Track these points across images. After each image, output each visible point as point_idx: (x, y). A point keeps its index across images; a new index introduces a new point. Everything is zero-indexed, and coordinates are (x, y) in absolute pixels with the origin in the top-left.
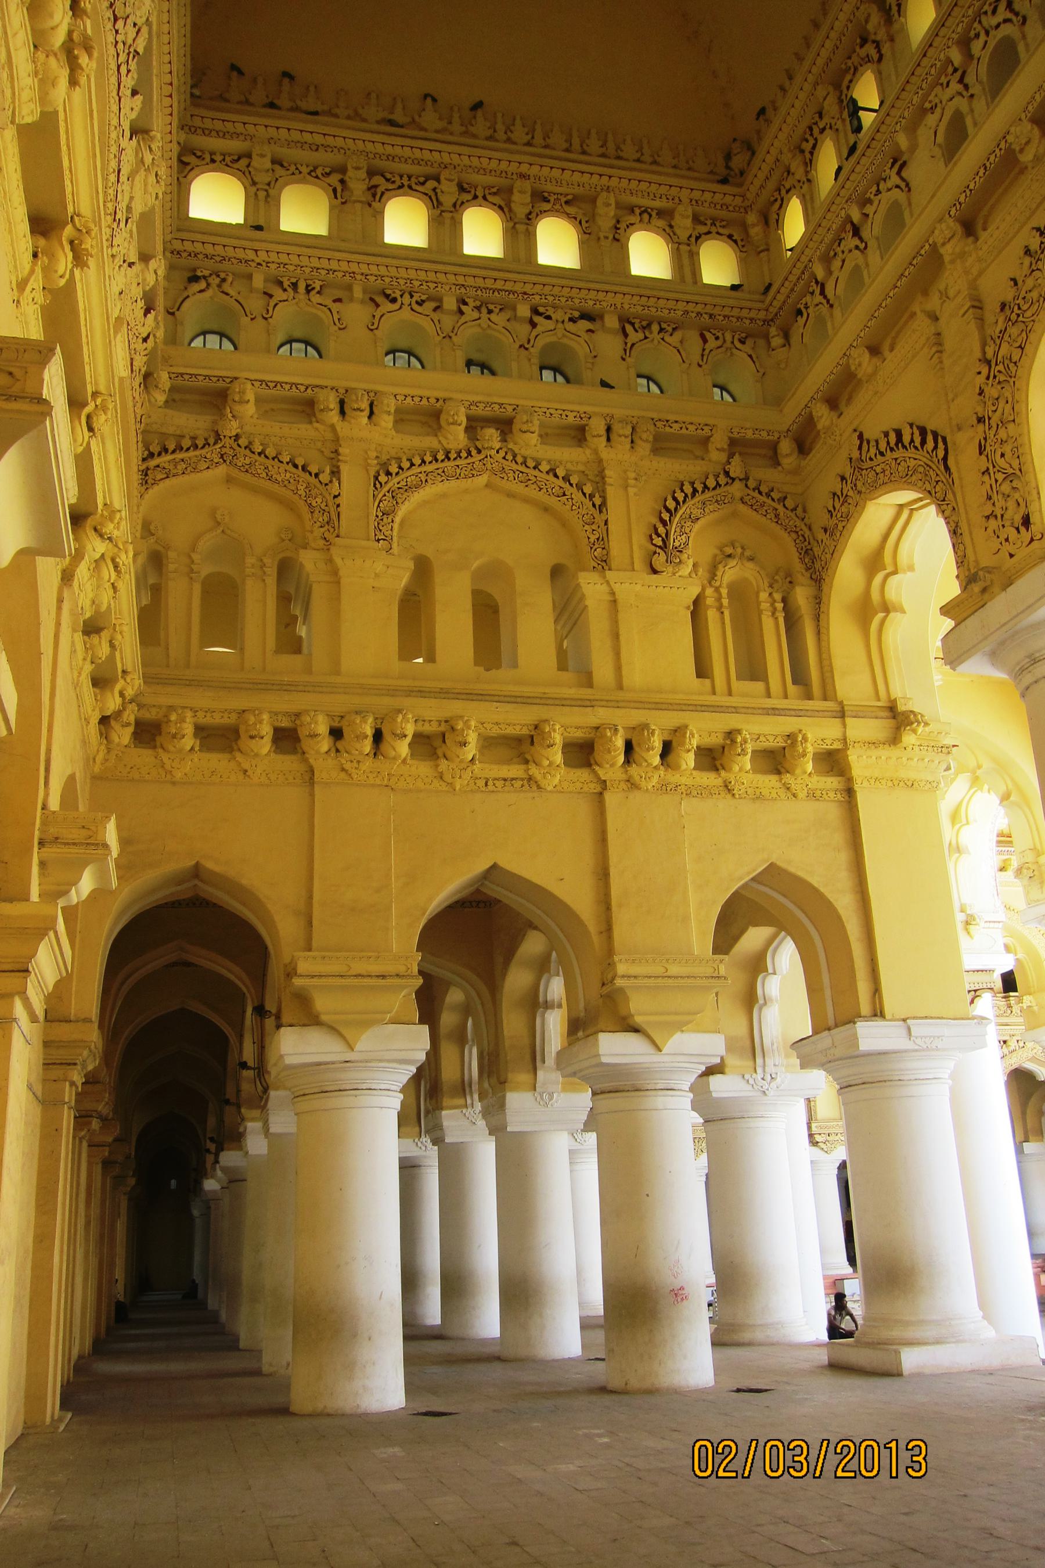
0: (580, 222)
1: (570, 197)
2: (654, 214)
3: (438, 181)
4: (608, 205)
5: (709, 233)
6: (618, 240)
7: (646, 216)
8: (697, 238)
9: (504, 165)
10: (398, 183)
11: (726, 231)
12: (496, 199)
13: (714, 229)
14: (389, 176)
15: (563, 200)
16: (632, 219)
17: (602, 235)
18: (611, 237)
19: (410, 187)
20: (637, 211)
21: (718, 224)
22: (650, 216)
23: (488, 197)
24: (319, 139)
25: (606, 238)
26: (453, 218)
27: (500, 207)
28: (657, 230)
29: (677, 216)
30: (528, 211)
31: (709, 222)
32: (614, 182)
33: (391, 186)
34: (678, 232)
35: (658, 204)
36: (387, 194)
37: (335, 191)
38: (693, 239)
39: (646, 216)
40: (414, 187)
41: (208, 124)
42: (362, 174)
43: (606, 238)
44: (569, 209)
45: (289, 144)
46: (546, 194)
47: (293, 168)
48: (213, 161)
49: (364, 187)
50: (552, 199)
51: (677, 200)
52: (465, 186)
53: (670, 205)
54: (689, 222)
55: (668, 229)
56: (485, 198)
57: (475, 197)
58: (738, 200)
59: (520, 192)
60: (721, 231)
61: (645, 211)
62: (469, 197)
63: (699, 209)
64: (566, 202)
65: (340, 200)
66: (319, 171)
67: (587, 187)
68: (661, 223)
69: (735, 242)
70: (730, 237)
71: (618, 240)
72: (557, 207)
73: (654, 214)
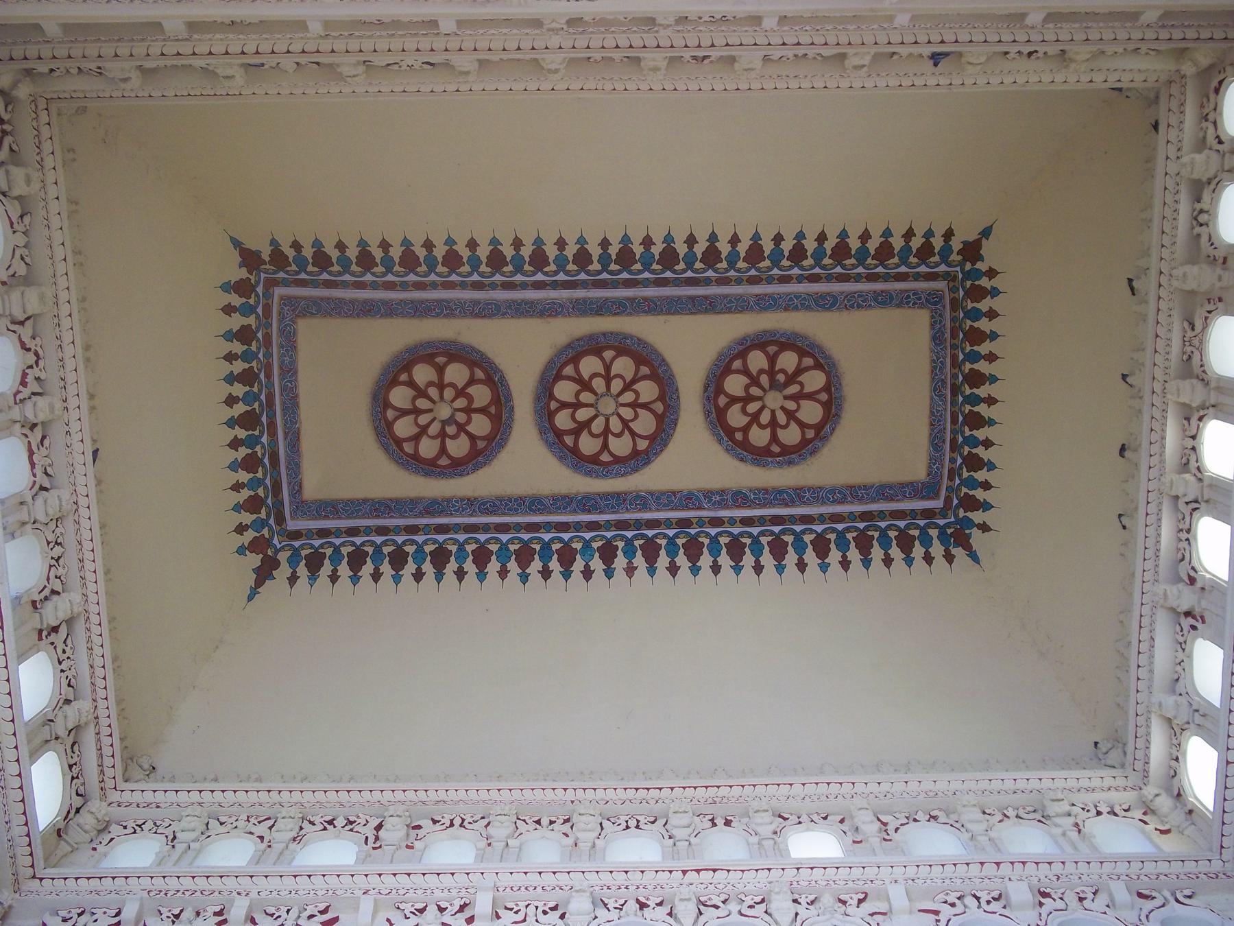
0: (1209, 312)
1: (1186, 324)
2: (1198, 206)
3: (1177, 498)
4: (1185, 275)
5: (1215, 123)
6: (1225, 259)
7: (1203, 218)
8: (1220, 142)
9: (1157, 414)
10: (1185, 544)
11: (1212, 96)
12: (1194, 421)
13: (1211, 117)
14: (1180, 556)
15: (1190, 334)
16: (1204, 239)
17: (1218, 285)
18: (1219, 271)
19: (1188, 531)
20: (1198, 230)
21: (1206, 111)
22: (1201, 211)
23: (1194, 432)
24: (1145, 635)
25: (1220, 278)
26: (1210, 486)
27: (1200, 419)
28: (1215, 202)
29: (1195, 176)
30: (1199, 385)
31: (1204, 124)
32: (1165, 267)
33: (1187, 558)
34: (1211, 174)
35: (1184, 208)
36: (1195, 563)
37: (1194, 628)
38: (1220, 147)
39: (1203, 218)
40: (1187, 526)
41: (1140, 754)
42: (1173, 590)
43: (1220, 278)
44: (1199, 325)
45: (1151, 671)
46: (1185, 357)
47: (1179, 668)
48: (1177, 759)
49: (1186, 590)
50: (1188, 349)
51: (1178, 179)
52: (1184, 460)
53: (1183, 189)
54: (1200, 158)
55: (1212, 186)
56: (1194, 437)
57: (1193, 449)
58: (1174, 89)
59: (1179, 396)
60: (1212, 106)
61: (1196, 219)
62: (1193, 458)
63: (1187, 144)
64: (1193, 329)
65: (1199, 625)
66: (1181, 639)
67: (1171, 304)
68: (1206, 196)
69: (1221, 83)
70: (1217, 91)
71: (1225, 259)
72: (1196, 342)
73: (1198, 206)
